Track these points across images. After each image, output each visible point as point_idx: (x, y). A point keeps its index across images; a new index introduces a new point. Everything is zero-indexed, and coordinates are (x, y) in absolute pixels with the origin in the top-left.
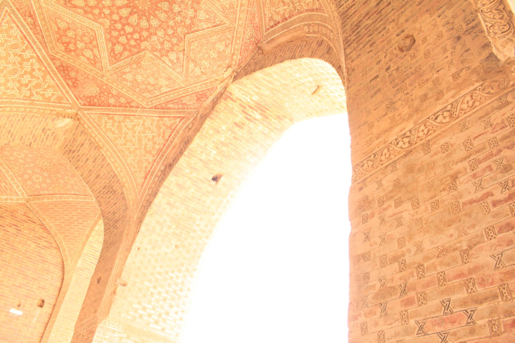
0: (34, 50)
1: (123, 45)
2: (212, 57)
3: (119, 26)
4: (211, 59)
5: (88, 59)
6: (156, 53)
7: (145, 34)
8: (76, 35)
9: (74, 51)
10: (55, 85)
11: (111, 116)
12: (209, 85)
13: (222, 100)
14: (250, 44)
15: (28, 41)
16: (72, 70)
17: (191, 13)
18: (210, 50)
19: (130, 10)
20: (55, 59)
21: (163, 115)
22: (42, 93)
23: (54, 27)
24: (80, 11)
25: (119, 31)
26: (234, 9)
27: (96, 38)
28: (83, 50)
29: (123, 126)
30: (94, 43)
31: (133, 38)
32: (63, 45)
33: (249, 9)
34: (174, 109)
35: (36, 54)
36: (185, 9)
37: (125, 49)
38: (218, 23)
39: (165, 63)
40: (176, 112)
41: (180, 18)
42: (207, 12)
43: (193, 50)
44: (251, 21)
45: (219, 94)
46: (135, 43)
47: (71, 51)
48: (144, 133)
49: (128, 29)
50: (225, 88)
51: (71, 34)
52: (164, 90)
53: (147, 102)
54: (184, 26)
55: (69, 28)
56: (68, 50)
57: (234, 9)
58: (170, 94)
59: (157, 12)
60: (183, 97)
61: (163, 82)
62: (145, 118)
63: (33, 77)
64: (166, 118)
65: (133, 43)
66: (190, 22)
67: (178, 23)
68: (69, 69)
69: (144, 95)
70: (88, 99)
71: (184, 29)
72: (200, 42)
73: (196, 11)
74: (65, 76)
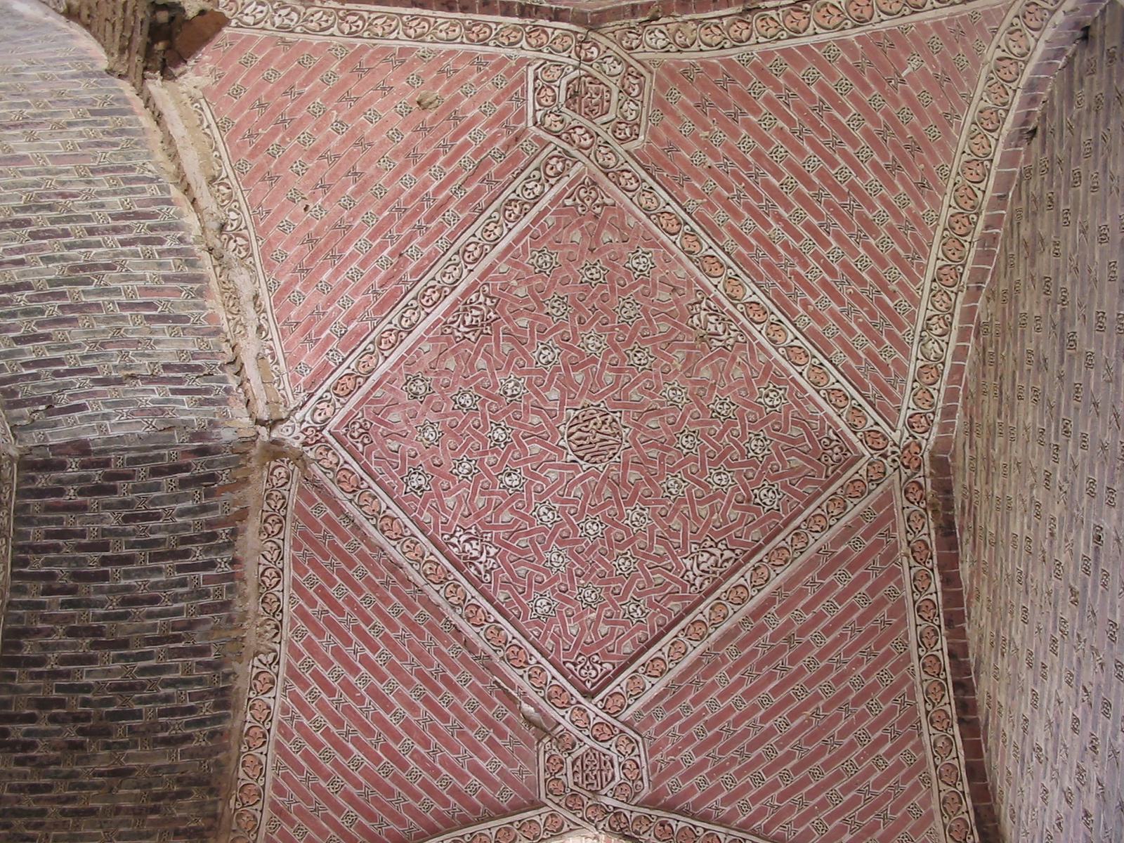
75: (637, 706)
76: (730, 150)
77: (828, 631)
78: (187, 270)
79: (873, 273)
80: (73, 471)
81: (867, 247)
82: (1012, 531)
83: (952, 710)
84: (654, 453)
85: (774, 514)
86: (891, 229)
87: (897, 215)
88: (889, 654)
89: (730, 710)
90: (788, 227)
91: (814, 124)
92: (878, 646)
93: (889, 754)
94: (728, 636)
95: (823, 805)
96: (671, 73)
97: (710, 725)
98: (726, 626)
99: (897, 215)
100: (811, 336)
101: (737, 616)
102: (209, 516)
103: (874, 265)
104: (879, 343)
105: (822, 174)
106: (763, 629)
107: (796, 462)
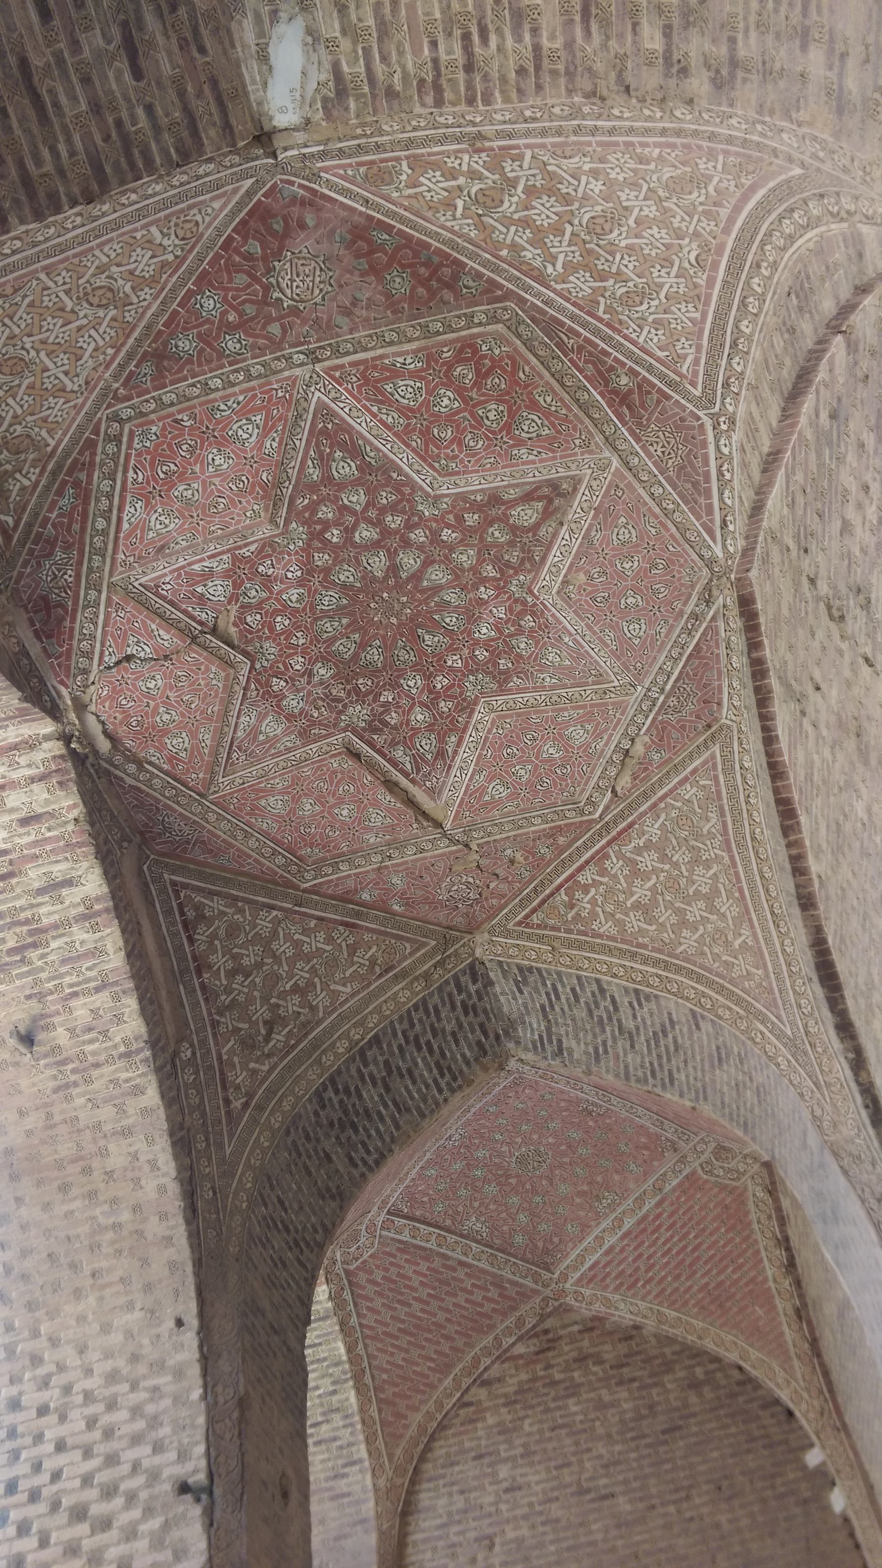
0: (568, 300)
1: (341, 486)
2: (161, 710)
3: (394, 522)
4: (157, 706)
5: (395, 373)
6: (252, 548)
7: (321, 559)
8: (479, 422)
9: (450, 366)
10: (429, 214)
11: (165, 276)
12: (83, 662)
13: (25, 705)
14: (150, 818)
15: (600, 320)
16: (412, 298)
17: (293, 703)
18: (183, 715)
19: (404, 576)
20: (487, 291)
21: (49, 468)
22: (461, 181)
23: (549, 399)
24: (513, 494)
25: (383, 511)
27: (425, 460)
28: (429, 393)
29: (101, 313)
30: (417, 441)
31: (337, 523)
32: (492, 360)
34: (54, 503)
35: (554, 291)
36: (310, 693)
37: (327, 479)
38: (235, 755)
39: (209, 557)
40: (37, 514)
41: (298, 667)
42: (272, 741)
43: (208, 669)
45: (42, 681)
46: (320, 515)
47: (459, 358)
48: (31, 387)
49: (365, 533)
50: (54, 712)
51: (491, 416)
52: (134, 512)
53: (121, 421)
54: (272, 667)
55: (508, 427)
56: (468, 351)
58: (108, 520)
59: (345, 621)
60: (80, 563)
61: (161, 523)
62: (80, 401)
63: (526, 223)
64: (33, 478)
65: (326, 512)
66: (275, 688)
67: (288, 656)
68: (421, 291)
69: (154, 429)
70: (278, 226)
71: (265, 664)
72: (216, 696)
73: (290, 717)
74: (416, 254)
75: (391, 1235)
76: (704, 1218)
77: (467, 1300)
78: (633, 1078)
80: (472, 988)
81: (665, 1277)
82: (571, 1401)
83: (464, 1386)
84: (528, 1186)
85: (512, 1245)
86: (677, 1289)
89: (410, 1279)
92: (472, 1329)
93: (429, 1368)
94: (444, 1256)
96: (741, 1195)
97: (399, 1275)
98: (449, 1253)
100: (612, 1248)
101: (458, 1255)
103: (657, 1279)
104: (616, 1278)
106: (454, 1270)
107: (540, 1244)
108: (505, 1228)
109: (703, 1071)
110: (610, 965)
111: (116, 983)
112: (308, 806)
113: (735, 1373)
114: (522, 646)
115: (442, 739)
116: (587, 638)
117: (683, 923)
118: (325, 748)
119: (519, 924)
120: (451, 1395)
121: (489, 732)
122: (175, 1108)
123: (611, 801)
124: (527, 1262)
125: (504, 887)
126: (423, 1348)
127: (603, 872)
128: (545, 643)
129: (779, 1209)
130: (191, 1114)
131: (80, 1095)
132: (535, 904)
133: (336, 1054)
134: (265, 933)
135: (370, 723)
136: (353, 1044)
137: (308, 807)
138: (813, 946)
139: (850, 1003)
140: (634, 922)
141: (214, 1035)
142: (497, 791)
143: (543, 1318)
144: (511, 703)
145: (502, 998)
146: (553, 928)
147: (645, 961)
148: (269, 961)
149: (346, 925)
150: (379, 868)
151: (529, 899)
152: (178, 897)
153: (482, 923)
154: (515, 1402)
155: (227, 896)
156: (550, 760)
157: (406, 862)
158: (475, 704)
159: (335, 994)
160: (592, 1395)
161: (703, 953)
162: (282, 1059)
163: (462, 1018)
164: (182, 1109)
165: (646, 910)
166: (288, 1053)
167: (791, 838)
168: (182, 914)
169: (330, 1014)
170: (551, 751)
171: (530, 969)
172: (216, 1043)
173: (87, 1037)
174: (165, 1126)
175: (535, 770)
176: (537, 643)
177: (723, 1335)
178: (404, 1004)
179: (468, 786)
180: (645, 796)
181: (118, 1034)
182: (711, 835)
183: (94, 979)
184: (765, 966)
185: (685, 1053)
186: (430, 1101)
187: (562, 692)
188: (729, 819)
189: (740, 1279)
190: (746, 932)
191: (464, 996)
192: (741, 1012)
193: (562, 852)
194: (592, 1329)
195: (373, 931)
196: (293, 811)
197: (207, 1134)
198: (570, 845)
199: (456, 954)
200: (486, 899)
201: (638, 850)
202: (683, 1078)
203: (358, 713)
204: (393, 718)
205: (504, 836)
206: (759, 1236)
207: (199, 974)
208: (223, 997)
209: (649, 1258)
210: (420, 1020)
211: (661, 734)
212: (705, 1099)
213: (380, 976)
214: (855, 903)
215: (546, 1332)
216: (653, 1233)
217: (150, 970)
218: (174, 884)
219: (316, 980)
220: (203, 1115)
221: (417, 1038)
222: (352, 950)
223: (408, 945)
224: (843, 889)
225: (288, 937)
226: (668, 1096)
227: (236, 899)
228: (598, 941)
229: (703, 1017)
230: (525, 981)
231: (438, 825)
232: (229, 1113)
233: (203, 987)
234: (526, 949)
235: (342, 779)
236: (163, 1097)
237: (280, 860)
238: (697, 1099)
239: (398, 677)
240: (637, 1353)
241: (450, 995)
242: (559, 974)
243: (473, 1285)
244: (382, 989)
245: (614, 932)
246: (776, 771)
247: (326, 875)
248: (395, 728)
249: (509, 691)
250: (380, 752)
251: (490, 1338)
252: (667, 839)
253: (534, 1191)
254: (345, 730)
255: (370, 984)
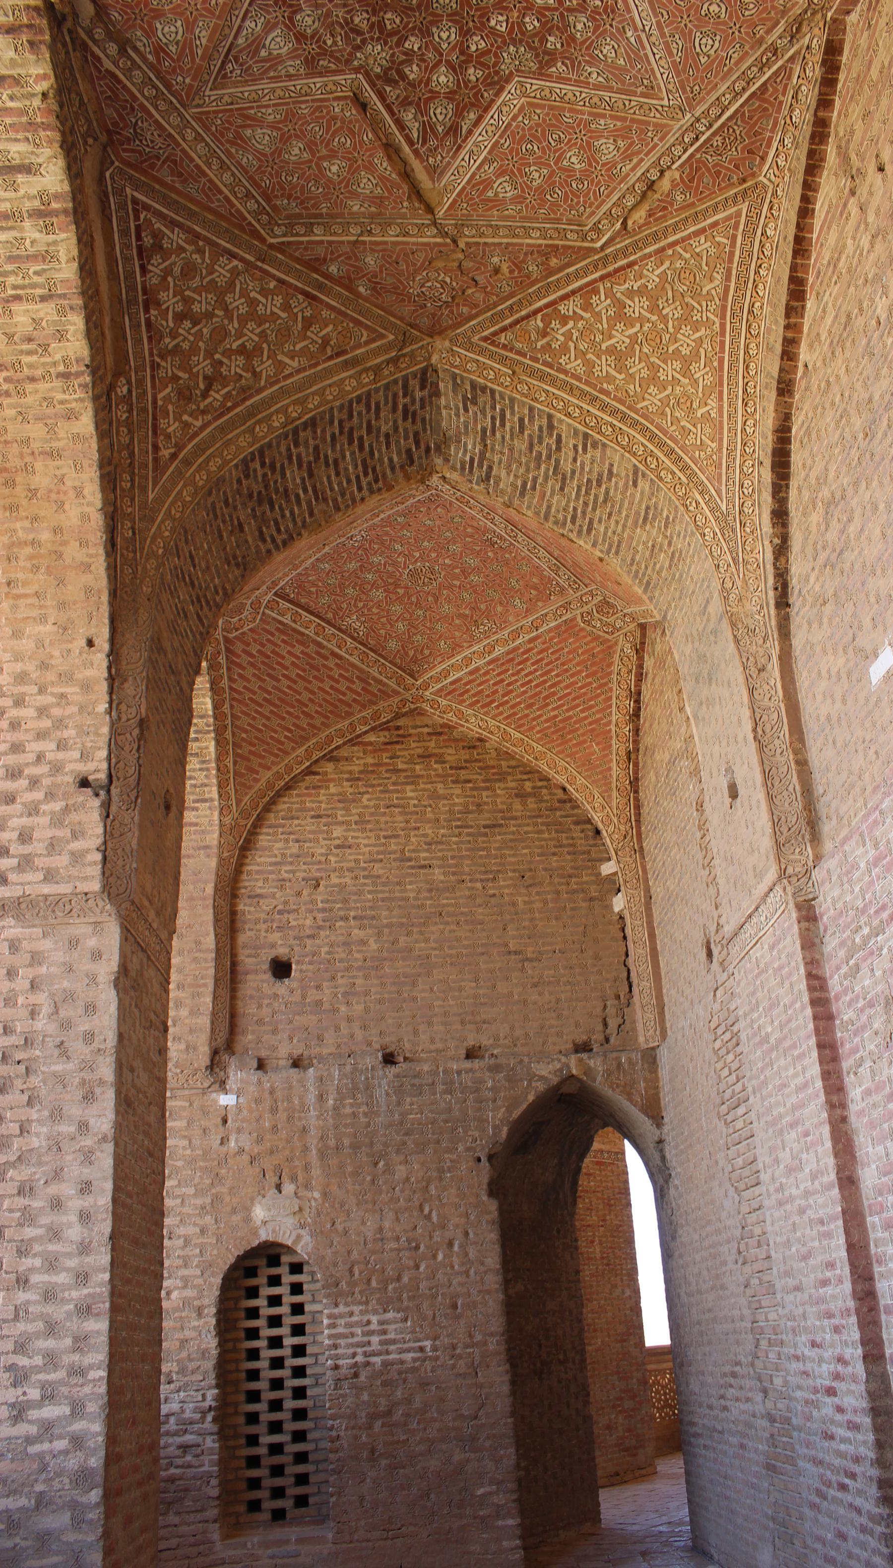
26: (228, 141)
33: (203, 180)
44: (175, 162)
57: (228, 141)
77: (332, 687)
78: (552, 519)
79: (507, 702)
80: (418, 394)
82: (408, 788)
83: (314, 758)
84: (414, 599)
85: (384, 648)
86: (527, 716)
87: (534, 719)
88: (328, 718)
89: (283, 658)
90: (530, 673)
91: (577, 698)
94: (320, 645)
95: (254, 718)
96: (610, 647)
97: (273, 652)
99: (534, 719)
100: (477, 669)
102: (388, 472)
104: (474, 696)
105: (554, 694)
106: (326, 659)
107: (411, 653)
108: (382, 632)
109: (624, 526)
110: (567, 404)
111: (64, 296)
112: (296, 151)
113: (560, 794)
114: (579, 27)
115: (459, 113)
116: (653, 39)
117: (653, 379)
118: (331, 86)
119: (485, 339)
120: (301, 763)
121: (514, 118)
122: (106, 441)
123: (619, 232)
124: (395, 665)
125: (479, 296)
126: (283, 719)
127: (587, 307)
128: (605, 31)
129: (640, 666)
130: (120, 452)
131: (11, 406)
132: (507, 322)
133: (270, 427)
134: (221, 282)
135: (386, 71)
136: (289, 421)
137: (296, 151)
138: (776, 431)
139: (793, 493)
140: (604, 366)
141: (153, 377)
142: (504, 189)
143: (398, 716)
144: (547, 92)
145: (444, 412)
146: (519, 353)
147: (603, 408)
148: (220, 313)
149: (307, 295)
150: (357, 241)
151: (501, 315)
152: (137, 218)
153: (446, 329)
154: (358, 779)
155: (189, 231)
156: (569, 170)
157: (386, 243)
158: (508, 80)
159: (280, 366)
160: (429, 786)
161: (663, 413)
162: (216, 419)
163: (400, 422)
164: (112, 445)
165: (619, 356)
166: (222, 414)
167: (792, 320)
168: (139, 238)
169: (272, 384)
170: (573, 159)
171: (484, 389)
172: (154, 387)
173: (25, 347)
174: (96, 456)
175: (551, 176)
176: (597, 28)
177: (557, 760)
178: (349, 393)
179: (474, 174)
180: (656, 237)
181: (58, 351)
182: (709, 297)
183: (42, 286)
184: (721, 440)
185: (613, 506)
186: (348, 496)
187: (606, 95)
188: (733, 285)
189: (586, 718)
190: (713, 403)
191: (408, 400)
192: (684, 479)
193: (551, 274)
194: (440, 734)
195: (332, 308)
196: (278, 152)
197: (132, 475)
198: (560, 269)
199: (412, 354)
200: (458, 305)
201: (630, 293)
202: (602, 530)
203: (377, 54)
204: (413, 72)
205: (496, 240)
206: (614, 686)
207: (147, 311)
208: (167, 340)
209: (509, 684)
210: (360, 414)
211: (694, 172)
212: (617, 553)
213: (331, 358)
214: (838, 398)
215: (398, 728)
216: (520, 663)
217: (97, 292)
218: (135, 201)
219: (265, 345)
220: (132, 455)
221: (351, 430)
222: (308, 323)
223: (365, 333)
224: (828, 383)
225: (244, 293)
226: (581, 543)
227: (197, 236)
228: (562, 376)
229: (644, 475)
230: (474, 402)
231: (430, 210)
232: (156, 460)
233: (148, 322)
234: (485, 367)
235: (341, 128)
236: (97, 427)
237: (252, 205)
238: (608, 552)
239: (432, 23)
240: (476, 761)
241: (395, 396)
242: (512, 400)
243: (341, 675)
244: (328, 372)
245: (581, 370)
246: (801, 246)
247: (297, 235)
248: (412, 84)
249: (548, 77)
250: (389, 108)
251: (347, 723)
252: (663, 288)
253: (418, 605)
254: (357, 70)
255: (317, 364)
